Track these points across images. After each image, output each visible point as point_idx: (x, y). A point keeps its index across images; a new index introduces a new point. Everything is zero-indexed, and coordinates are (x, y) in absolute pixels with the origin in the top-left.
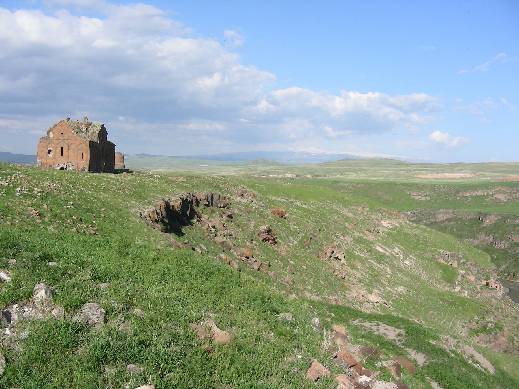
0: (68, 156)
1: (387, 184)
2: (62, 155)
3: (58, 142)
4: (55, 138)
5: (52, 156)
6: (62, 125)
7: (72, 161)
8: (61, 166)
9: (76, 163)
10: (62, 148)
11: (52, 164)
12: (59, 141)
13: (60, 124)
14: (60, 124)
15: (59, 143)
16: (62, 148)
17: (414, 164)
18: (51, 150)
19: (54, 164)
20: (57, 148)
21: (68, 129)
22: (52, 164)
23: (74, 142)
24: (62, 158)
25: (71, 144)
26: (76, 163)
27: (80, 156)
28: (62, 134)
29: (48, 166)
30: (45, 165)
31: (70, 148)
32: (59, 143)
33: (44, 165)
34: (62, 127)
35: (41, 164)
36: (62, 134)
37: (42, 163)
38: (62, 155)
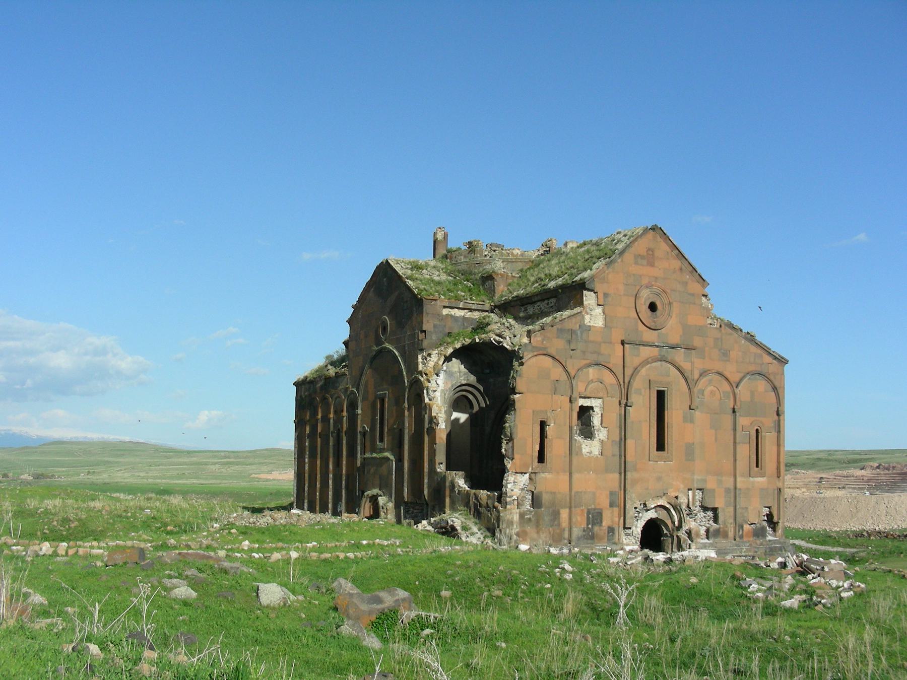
0: (689, 452)
1: (271, 494)
2: (661, 446)
3: (637, 361)
4: (618, 336)
5: (596, 451)
6: (650, 250)
7: (711, 484)
8: (652, 514)
9: (727, 491)
10: (661, 395)
11: (603, 501)
12: (646, 352)
13: (641, 247)
14: (641, 247)
15: (646, 362)
16: (661, 395)
17: (195, 452)
18: (592, 408)
19: (612, 505)
20: (633, 398)
21: (685, 284)
22: (603, 501)
23: (719, 367)
24: (660, 465)
25: (703, 374)
26: (727, 491)
27: (745, 452)
28: (653, 307)
29: (580, 521)
30: (564, 514)
31: (697, 401)
32: (646, 362)
33: (556, 515)
34: (651, 264)
35: (536, 501)
36: (653, 307)
37: (546, 498)
38: (661, 446)
